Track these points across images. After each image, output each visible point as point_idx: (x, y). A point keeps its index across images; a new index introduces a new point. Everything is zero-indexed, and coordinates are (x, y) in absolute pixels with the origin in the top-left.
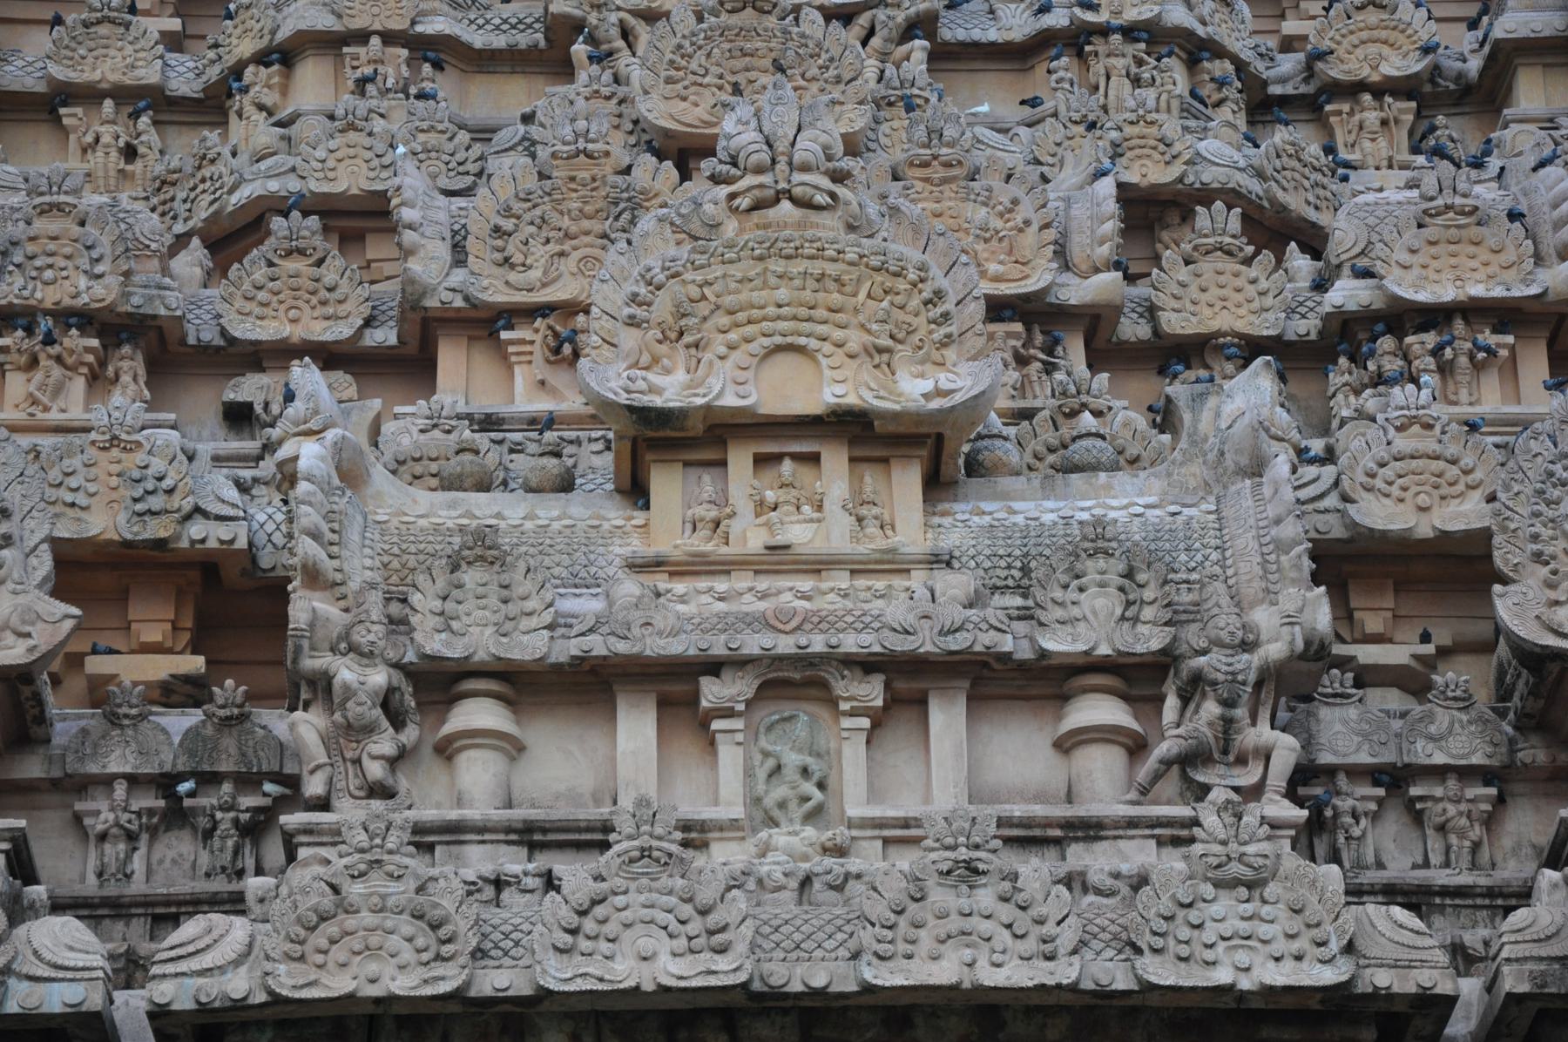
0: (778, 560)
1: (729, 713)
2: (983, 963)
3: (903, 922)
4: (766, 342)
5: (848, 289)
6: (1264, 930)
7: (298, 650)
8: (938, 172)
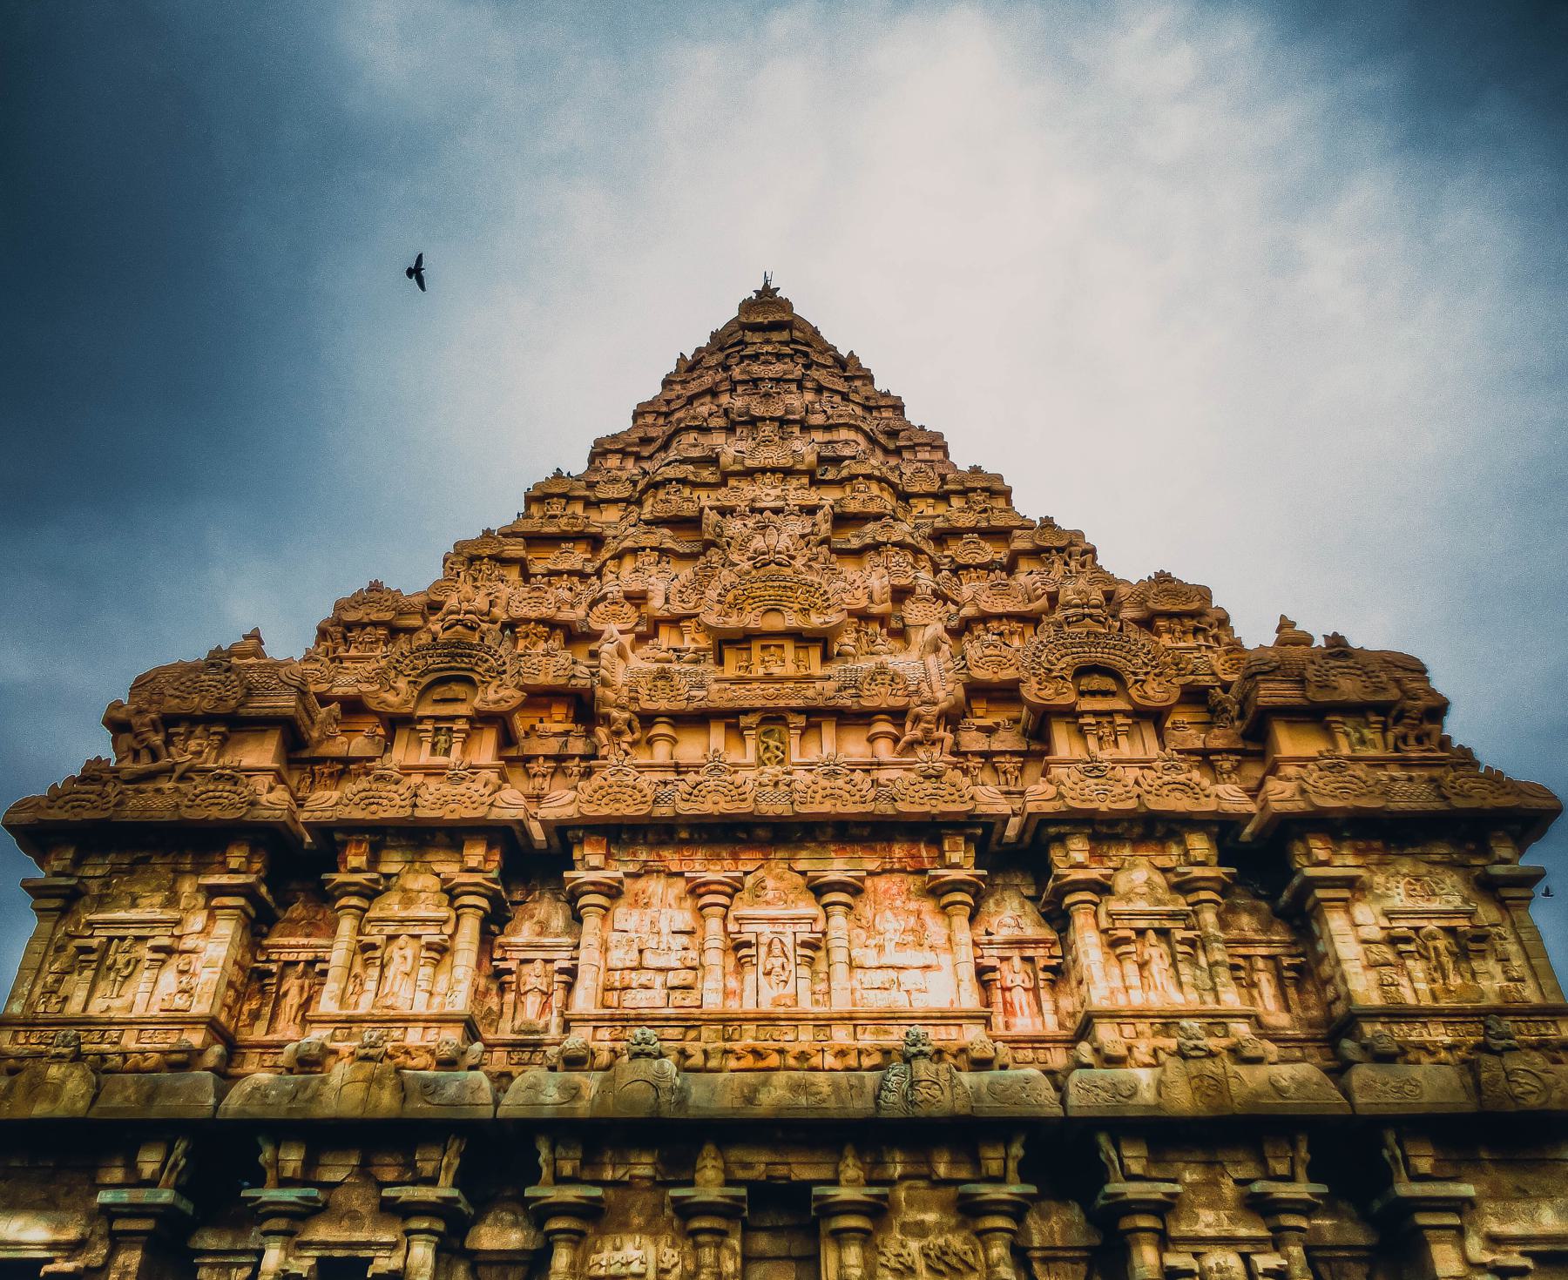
0: (769, 678)
1: (751, 728)
2: (839, 804)
3: (810, 791)
6: (941, 792)
7: (598, 706)
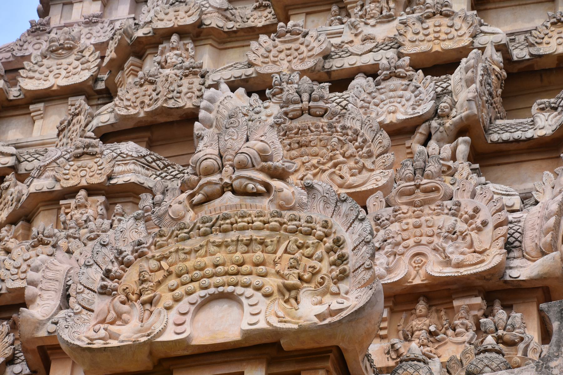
4: (203, 293)
5: (270, 248)
8: (420, 196)
